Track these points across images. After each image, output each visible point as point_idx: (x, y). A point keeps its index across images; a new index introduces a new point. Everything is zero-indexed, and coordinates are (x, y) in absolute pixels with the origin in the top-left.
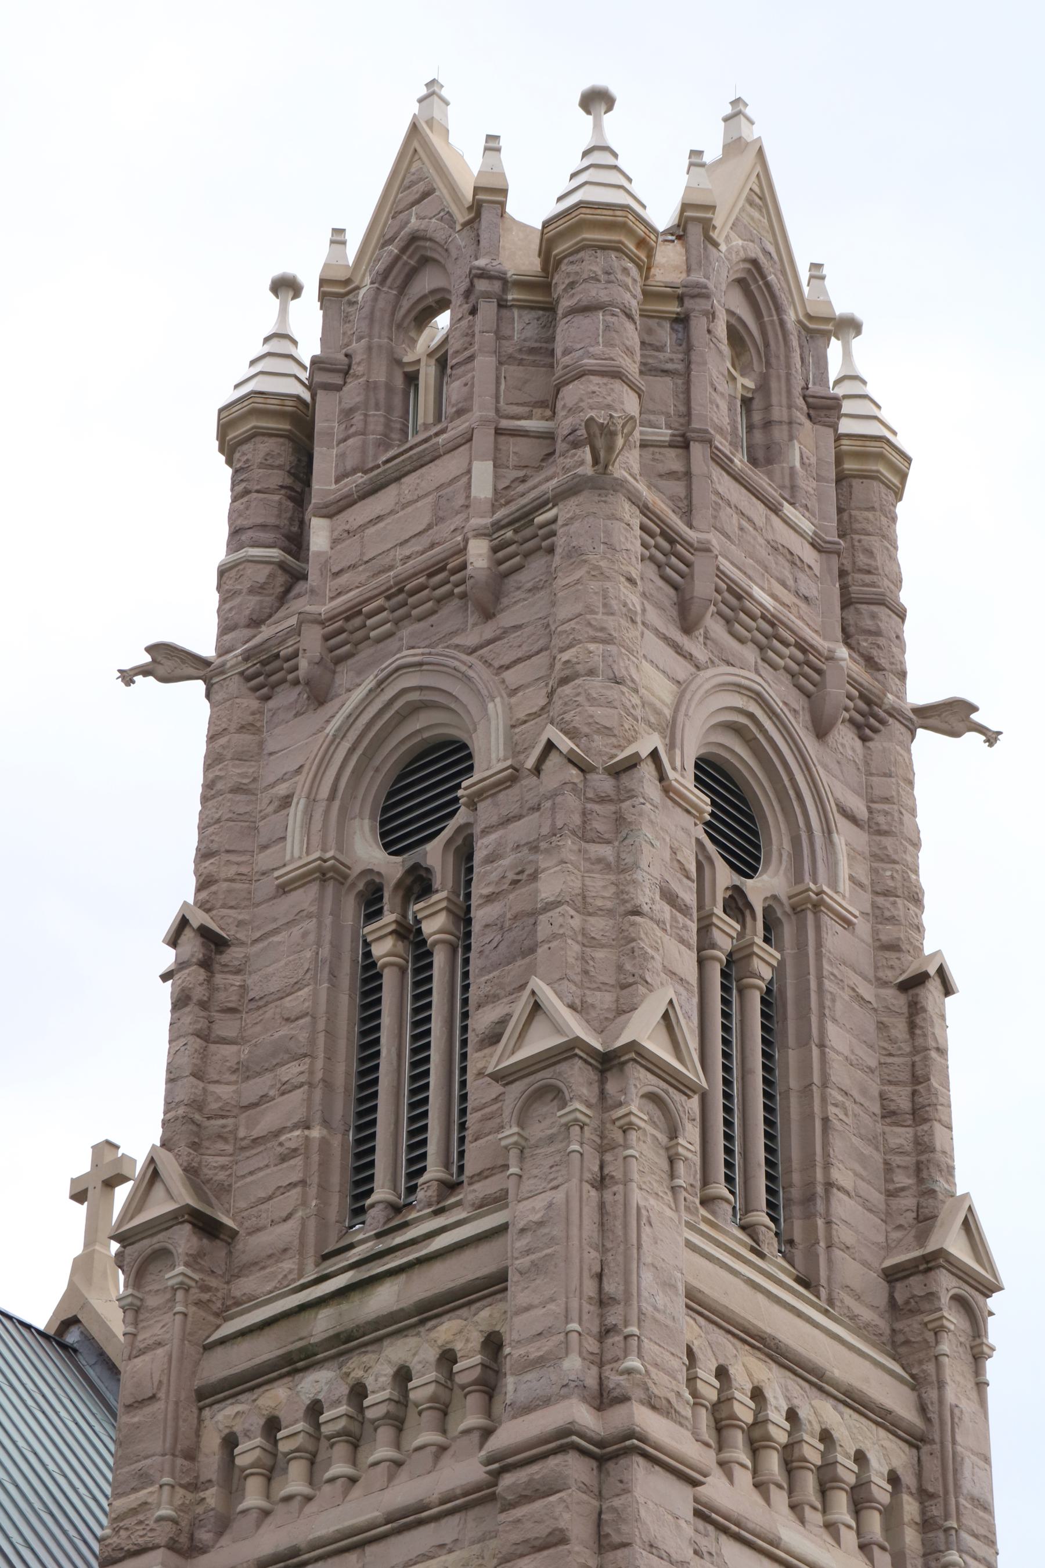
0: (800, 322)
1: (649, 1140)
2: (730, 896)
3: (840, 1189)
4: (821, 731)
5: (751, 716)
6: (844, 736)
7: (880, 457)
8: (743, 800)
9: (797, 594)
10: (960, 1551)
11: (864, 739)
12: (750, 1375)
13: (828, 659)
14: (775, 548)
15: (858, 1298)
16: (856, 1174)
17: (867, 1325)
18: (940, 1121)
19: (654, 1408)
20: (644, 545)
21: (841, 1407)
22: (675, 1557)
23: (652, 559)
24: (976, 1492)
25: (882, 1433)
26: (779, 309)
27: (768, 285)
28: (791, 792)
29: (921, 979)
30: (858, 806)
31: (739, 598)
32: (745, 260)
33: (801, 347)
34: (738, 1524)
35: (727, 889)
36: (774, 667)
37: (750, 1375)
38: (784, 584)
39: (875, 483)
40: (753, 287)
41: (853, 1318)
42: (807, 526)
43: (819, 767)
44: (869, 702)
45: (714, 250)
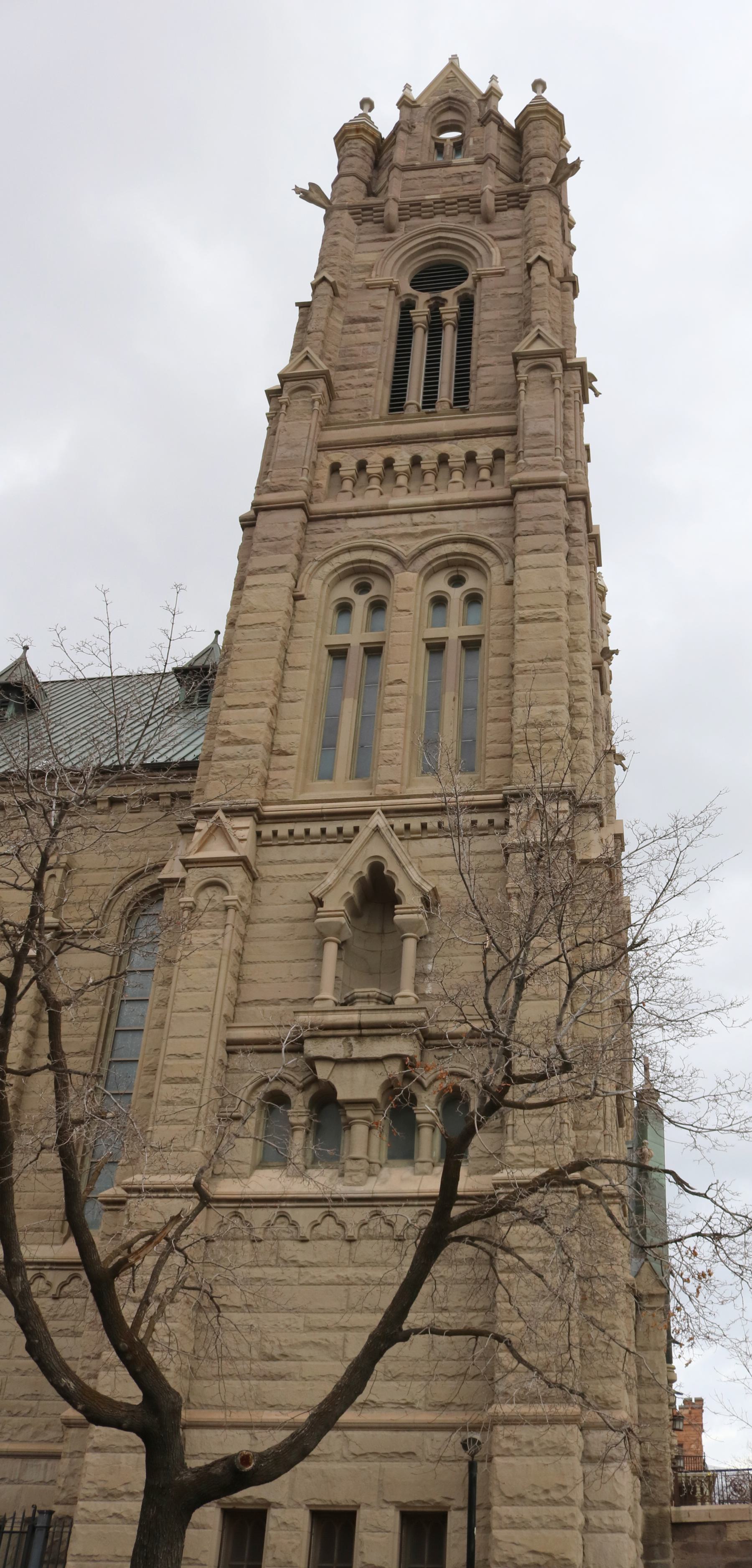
0: (479, 100)
1: (300, 404)
2: (436, 302)
3: (484, 366)
4: (487, 221)
5: (439, 238)
6: (511, 214)
7: (529, 113)
8: (459, 268)
9: (464, 184)
10: (524, 458)
11: (523, 208)
12: (381, 455)
13: (482, 194)
14: (448, 178)
15: (494, 398)
16: (498, 356)
17: (499, 405)
18: (536, 310)
19: (275, 491)
20: (354, 219)
21: (455, 441)
22: (280, 537)
23: (364, 221)
24: (535, 431)
25: (488, 439)
26: (465, 103)
27: (459, 101)
28: (470, 250)
29: (529, 267)
30: (518, 231)
31: (419, 204)
32: (443, 100)
33: (480, 107)
34: (357, 511)
35: (428, 301)
36: (455, 215)
37: (381, 455)
38: (453, 185)
39: (531, 124)
40: (455, 106)
41: (488, 407)
42: (471, 159)
43: (481, 232)
44: (516, 194)
45: (417, 109)
